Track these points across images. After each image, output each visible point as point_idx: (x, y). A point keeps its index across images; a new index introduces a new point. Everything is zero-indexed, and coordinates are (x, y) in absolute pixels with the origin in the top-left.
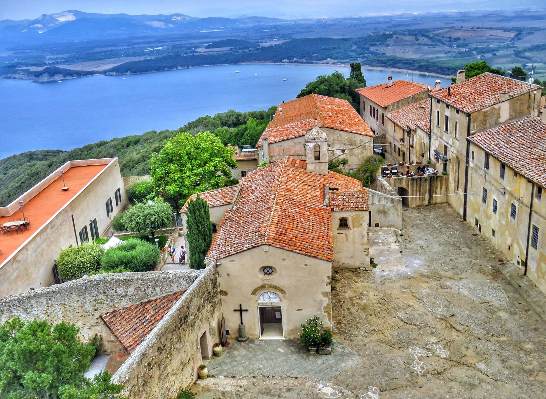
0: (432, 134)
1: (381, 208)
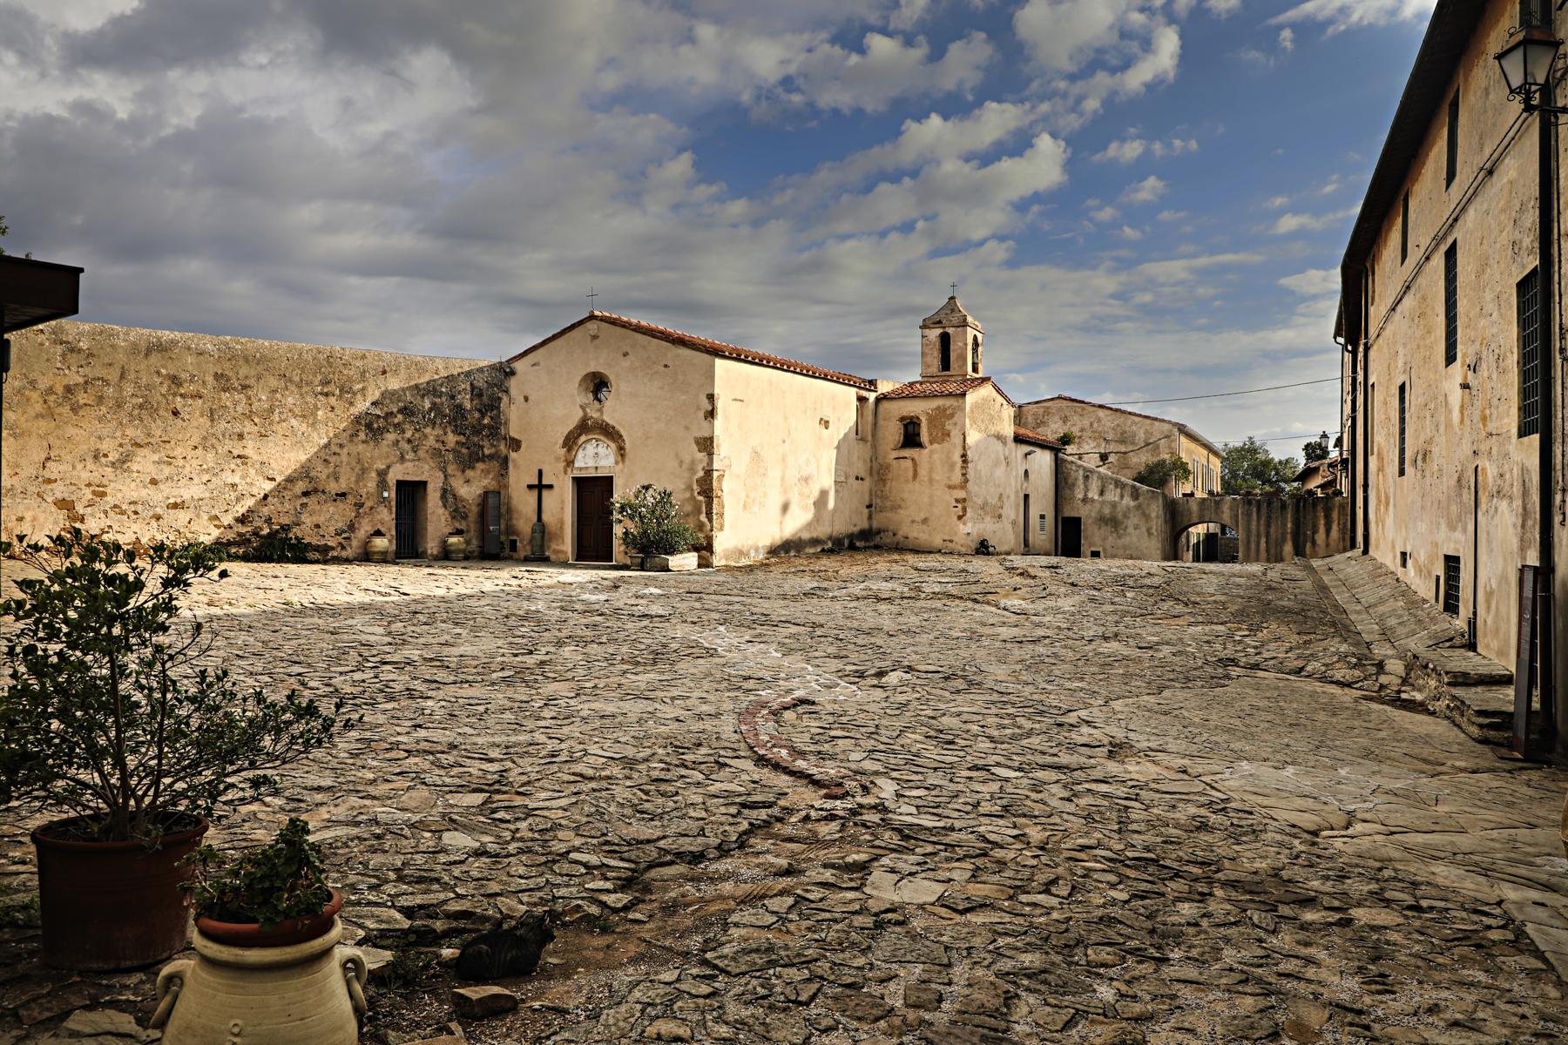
1: (1107, 511)
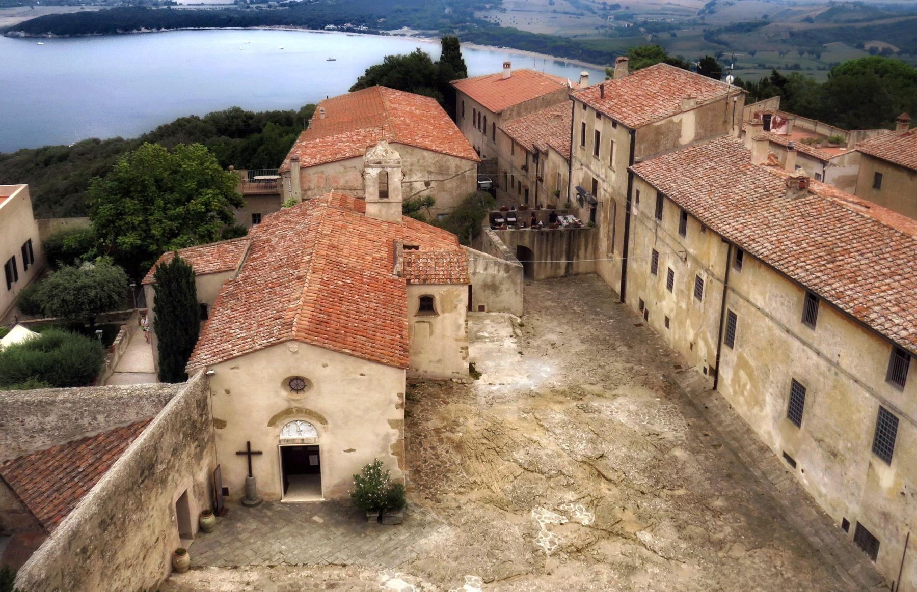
0: (573, 160)
1: (489, 281)
